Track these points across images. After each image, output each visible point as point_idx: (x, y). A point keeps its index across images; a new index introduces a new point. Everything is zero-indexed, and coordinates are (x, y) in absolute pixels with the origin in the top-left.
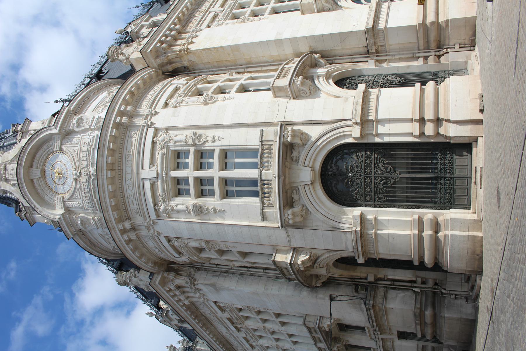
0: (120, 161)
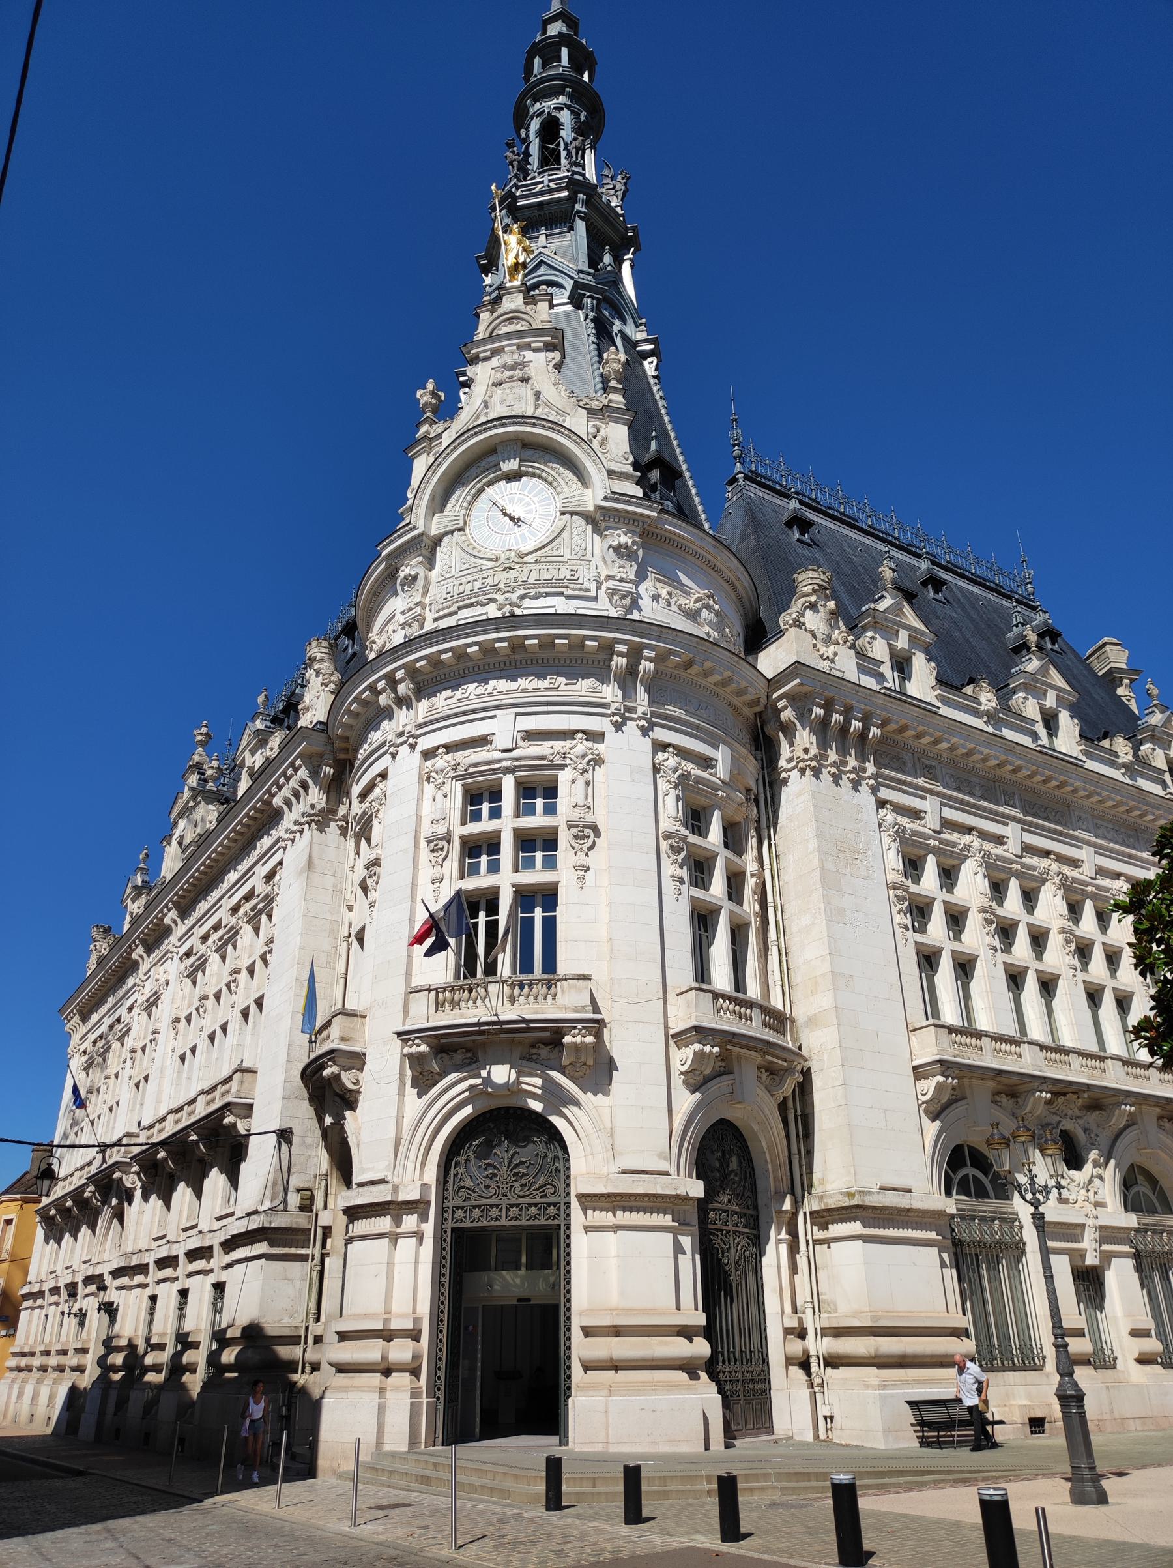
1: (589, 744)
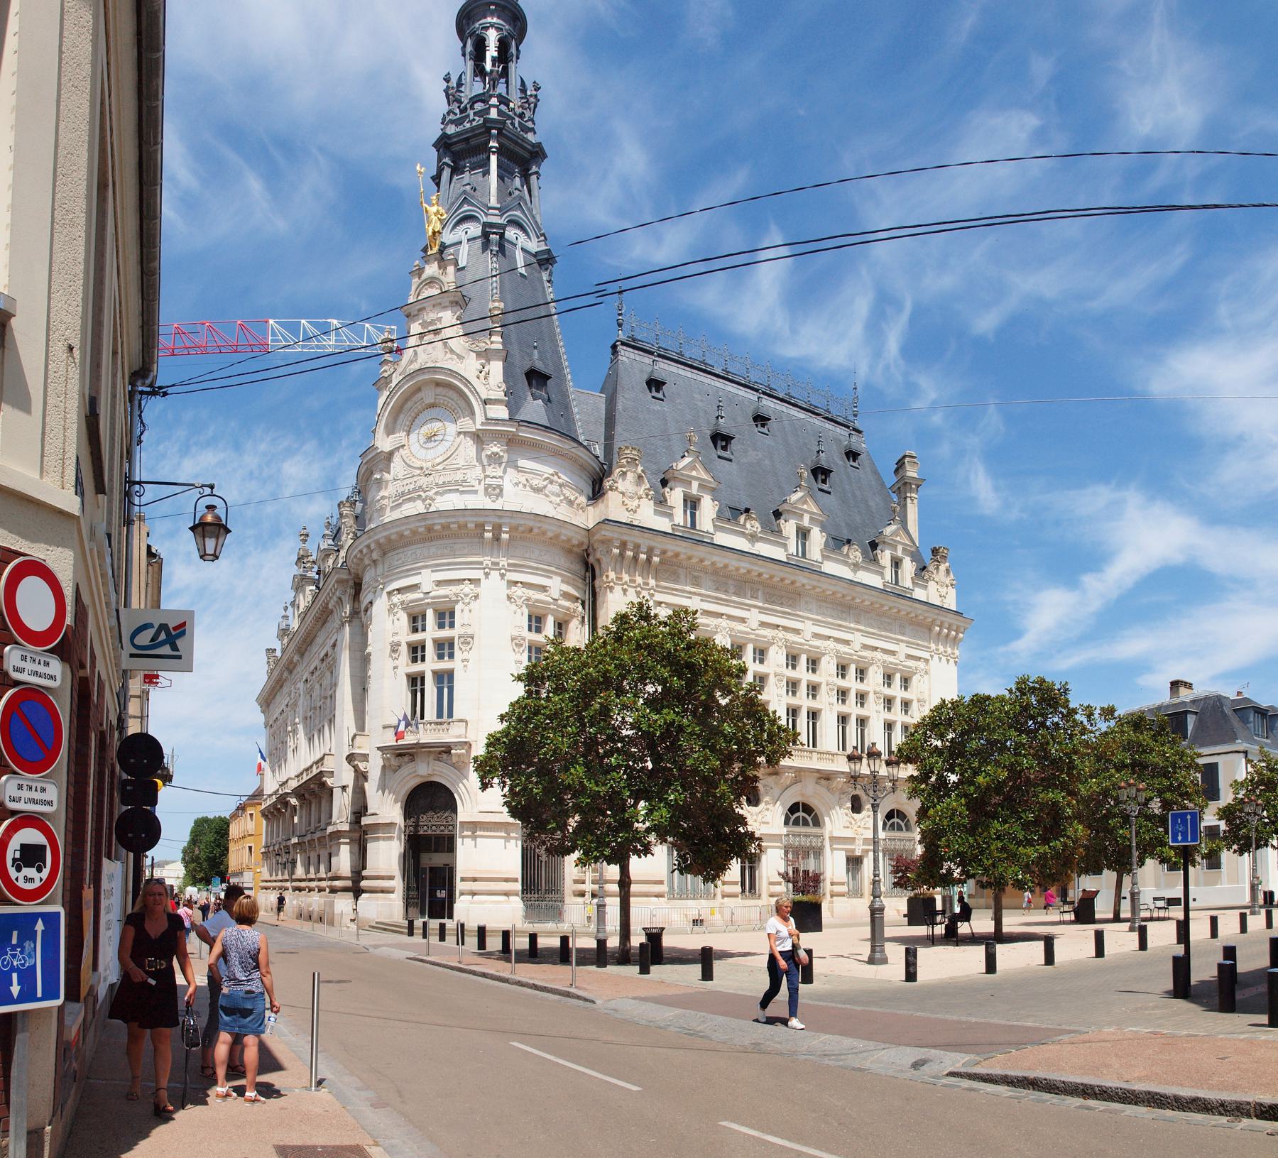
0: (440, 538)
1: (472, 586)
